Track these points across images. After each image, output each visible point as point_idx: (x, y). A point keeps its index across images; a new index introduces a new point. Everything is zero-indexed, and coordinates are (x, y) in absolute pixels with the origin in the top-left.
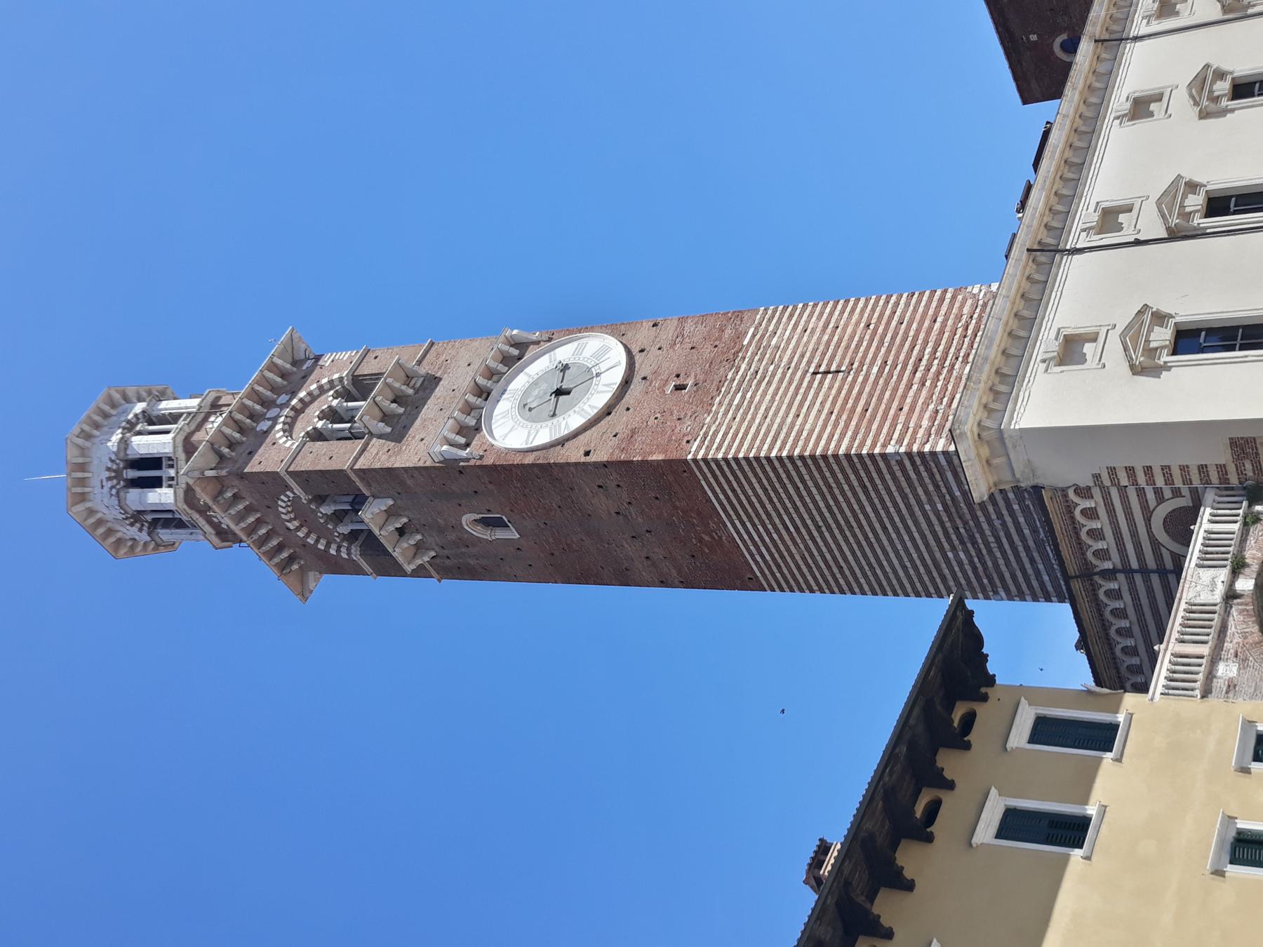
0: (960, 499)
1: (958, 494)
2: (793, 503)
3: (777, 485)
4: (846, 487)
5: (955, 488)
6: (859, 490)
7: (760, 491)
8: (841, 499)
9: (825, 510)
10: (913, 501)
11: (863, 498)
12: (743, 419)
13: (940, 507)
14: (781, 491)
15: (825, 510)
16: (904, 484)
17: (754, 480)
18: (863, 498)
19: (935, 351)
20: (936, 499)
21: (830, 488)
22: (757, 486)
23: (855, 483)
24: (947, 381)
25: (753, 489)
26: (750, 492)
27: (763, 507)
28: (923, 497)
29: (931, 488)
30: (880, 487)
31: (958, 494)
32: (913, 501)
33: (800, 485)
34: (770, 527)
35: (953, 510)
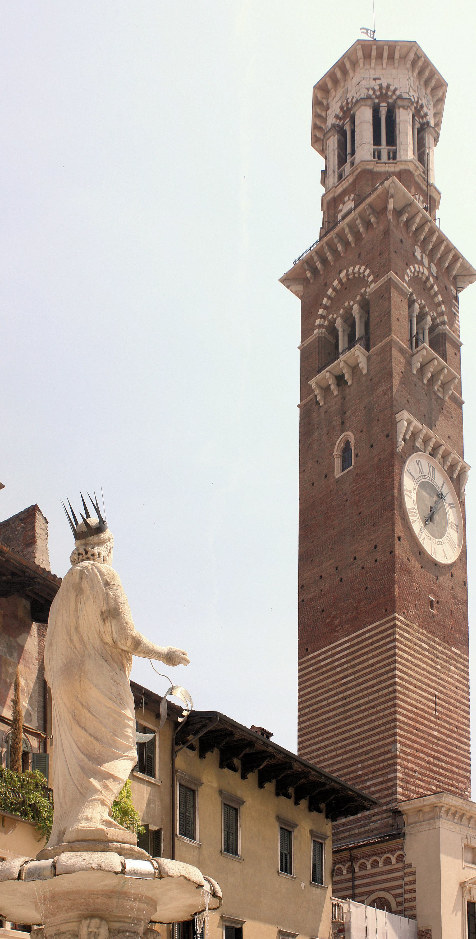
0: (365, 785)
1: (368, 783)
2: (363, 683)
3: (375, 674)
4: (373, 717)
5: (372, 782)
6: (372, 725)
7: (371, 662)
8: (366, 713)
9: (357, 703)
10: (363, 757)
11: (366, 727)
12: (414, 650)
13: (360, 773)
14: (372, 675)
15: (357, 703)
16: (375, 753)
17: (379, 658)
18: (366, 727)
19: (443, 768)
20: (365, 771)
21: (373, 707)
22: (375, 660)
23: (376, 723)
24: (429, 776)
25: (373, 657)
26: (370, 655)
27: (360, 663)
28: (366, 764)
29: (373, 768)
30: (373, 739)
31: (368, 783)
32: (363, 757)
33: (375, 689)
34: (345, 666)
35: (358, 780)
